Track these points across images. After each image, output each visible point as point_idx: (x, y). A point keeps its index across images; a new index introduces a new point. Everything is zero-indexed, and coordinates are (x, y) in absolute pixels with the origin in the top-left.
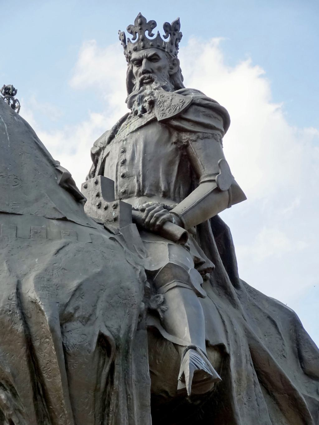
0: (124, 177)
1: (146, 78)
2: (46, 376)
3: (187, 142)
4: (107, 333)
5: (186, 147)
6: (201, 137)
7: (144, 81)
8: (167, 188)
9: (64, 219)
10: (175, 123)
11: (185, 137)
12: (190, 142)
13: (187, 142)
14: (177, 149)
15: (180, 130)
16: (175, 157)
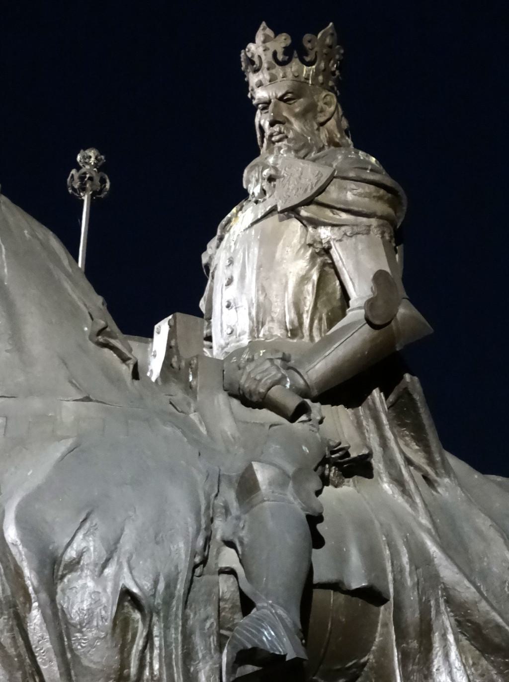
0: (230, 308)
1: (276, 133)
2: (40, 660)
3: (328, 242)
4: (135, 590)
5: (327, 251)
6: (348, 234)
7: (273, 139)
8: (296, 323)
9: (87, 399)
10: (304, 213)
11: (325, 233)
12: (332, 243)
13: (328, 242)
14: (313, 257)
15: (315, 223)
16: (310, 269)
